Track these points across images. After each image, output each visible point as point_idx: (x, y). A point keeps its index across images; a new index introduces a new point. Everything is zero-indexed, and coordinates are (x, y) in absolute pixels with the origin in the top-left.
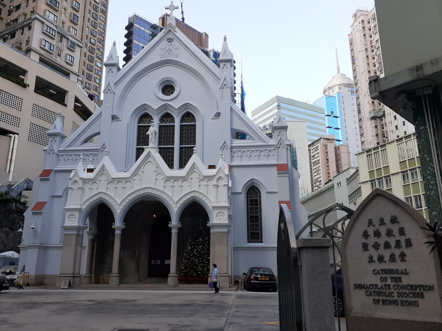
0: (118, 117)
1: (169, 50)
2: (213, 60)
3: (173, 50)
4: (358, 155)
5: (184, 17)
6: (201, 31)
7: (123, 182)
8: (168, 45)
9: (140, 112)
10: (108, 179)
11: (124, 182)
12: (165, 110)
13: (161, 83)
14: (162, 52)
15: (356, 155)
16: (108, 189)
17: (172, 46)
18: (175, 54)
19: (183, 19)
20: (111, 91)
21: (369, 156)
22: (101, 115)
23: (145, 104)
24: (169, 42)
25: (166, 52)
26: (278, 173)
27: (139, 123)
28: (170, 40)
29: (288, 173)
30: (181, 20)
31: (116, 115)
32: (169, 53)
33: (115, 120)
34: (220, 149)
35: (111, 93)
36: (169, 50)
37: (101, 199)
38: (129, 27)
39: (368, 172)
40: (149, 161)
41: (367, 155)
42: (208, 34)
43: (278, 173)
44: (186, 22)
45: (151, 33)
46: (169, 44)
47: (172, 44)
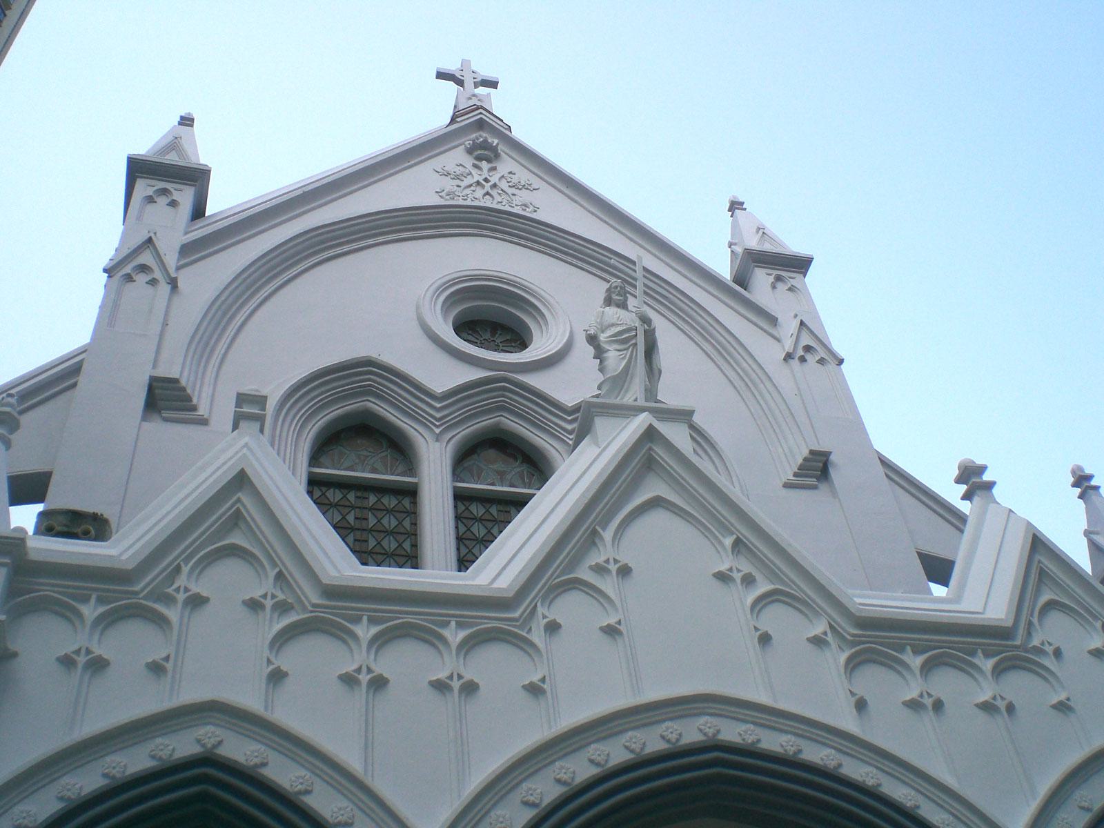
0: (189, 399)
1: (488, 185)
3: (504, 185)
7: (446, 633)
8: (475, 166)
9: (345, 398)
10: (281, 596)
11: (454, 635)
12: (489, 411)
13: (452, 293)
14: (449, 184)
16: (289, 685)
17: (494, 179)
18: (517, 200)
20: (158, 274)
22: (75, 385)
23: (369, 362)
24: (479, 158)
25: (472, 188)
27: (314, 459)
28: (485, 153)
31: (183, 382)
32: (487, 193)
33: (165, 414)
35: (153, 282)
36: (488, 185)
37: (206, 779)
40: (656, 503)
46: (484, 165)
47: (494, 169)
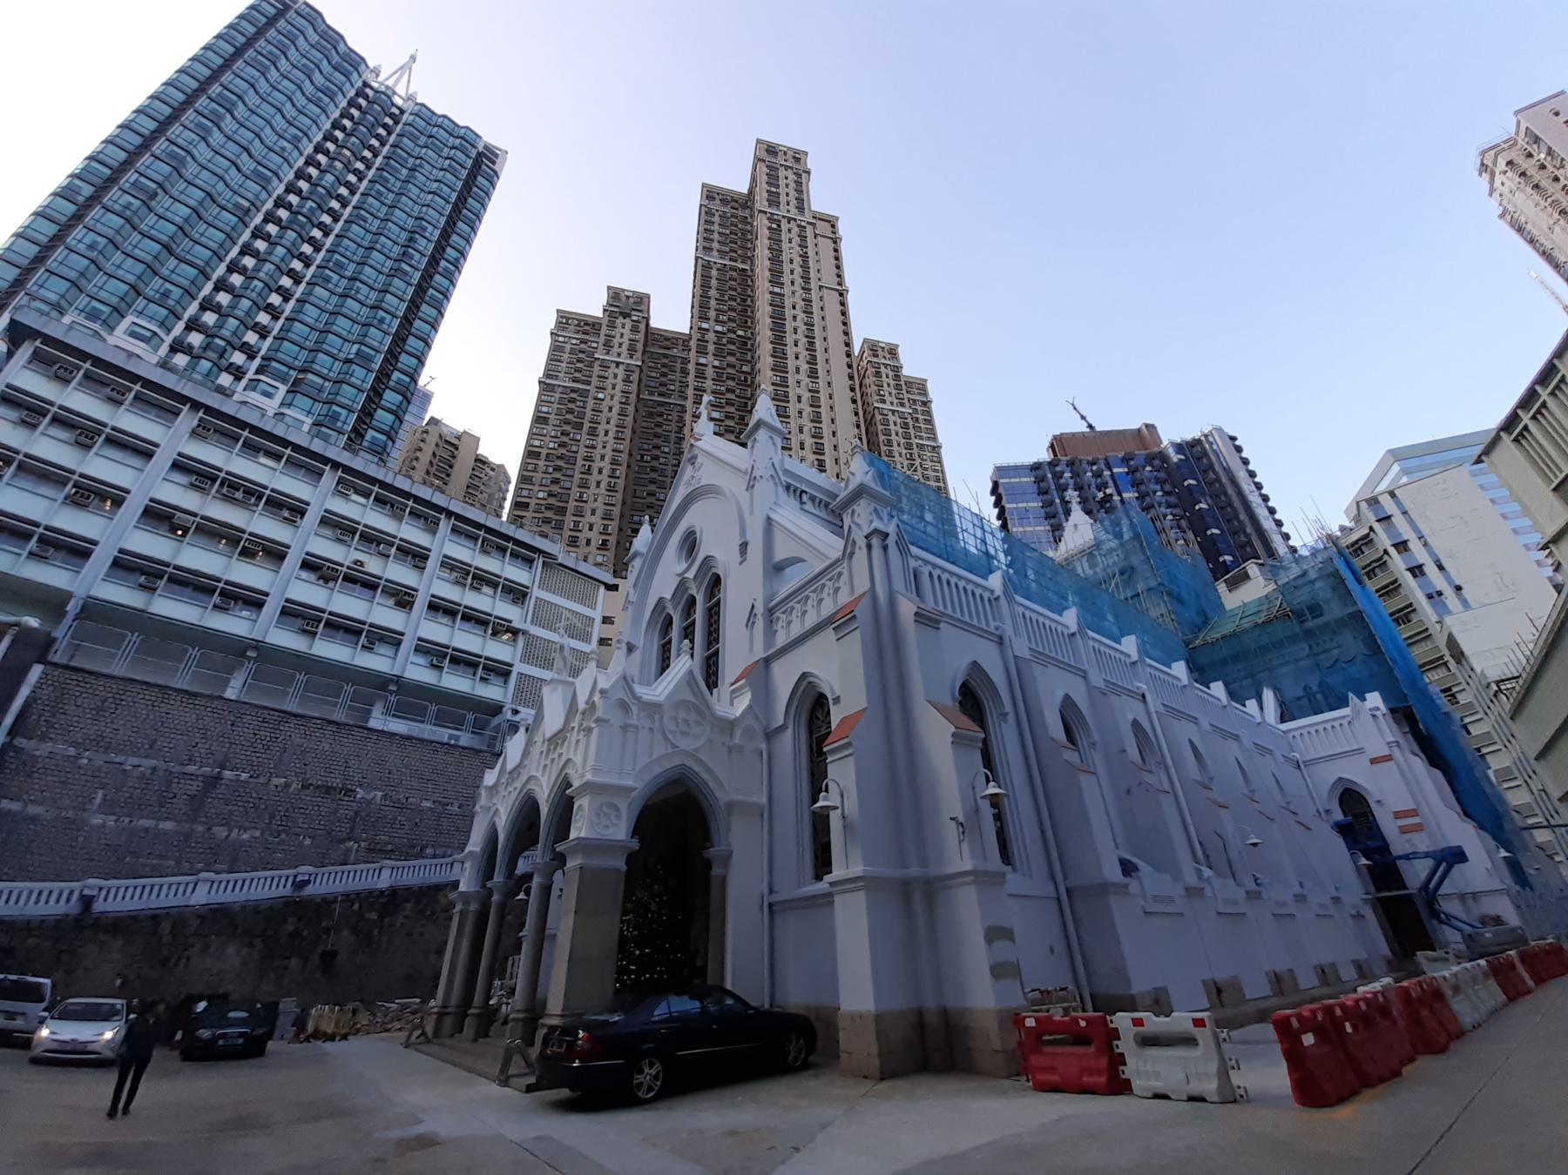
2: (1180, 460)
4: (1483, 458)
5: (1090, 422)
6: (1136, 426)
15: (1479, 461)
19: (1090, 426)
21: (1525, 438)
26: (834, 629)
29: (854, 616)
30: (1088, 430)
34: (747, 626)
38: (995, 490)
39: (1551, 494)
41: (1516, 440)
42: (1151, 422)
43: (834, 629)
44: (1098, 428)
45: (1033, 479)
